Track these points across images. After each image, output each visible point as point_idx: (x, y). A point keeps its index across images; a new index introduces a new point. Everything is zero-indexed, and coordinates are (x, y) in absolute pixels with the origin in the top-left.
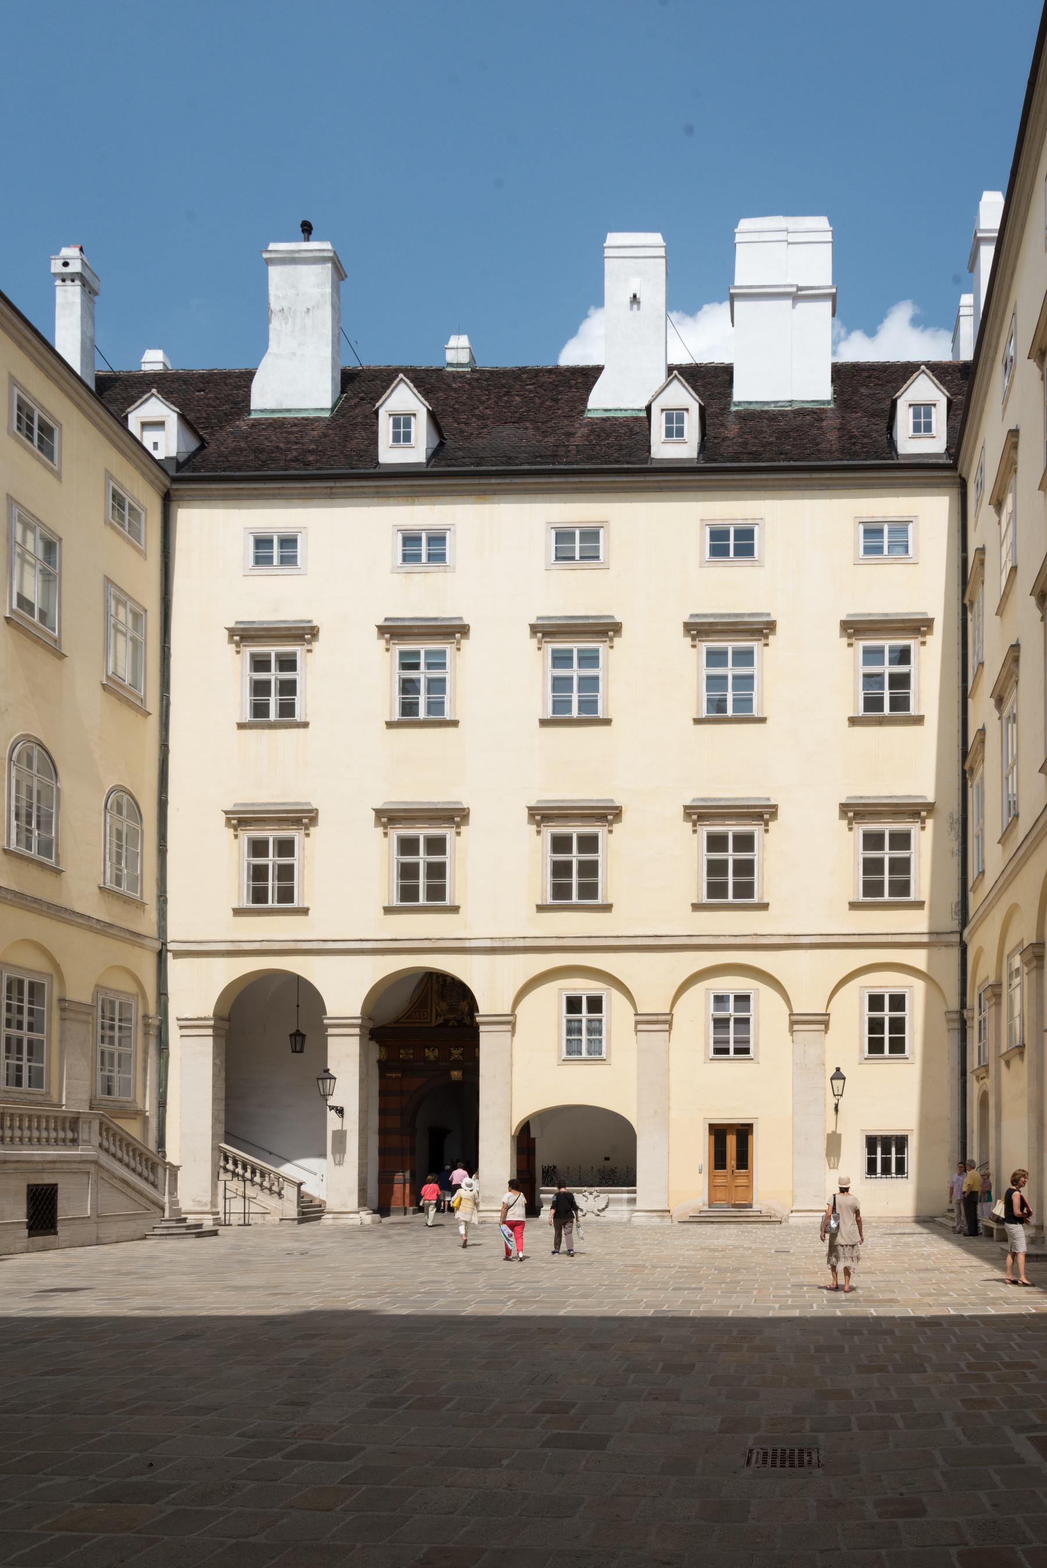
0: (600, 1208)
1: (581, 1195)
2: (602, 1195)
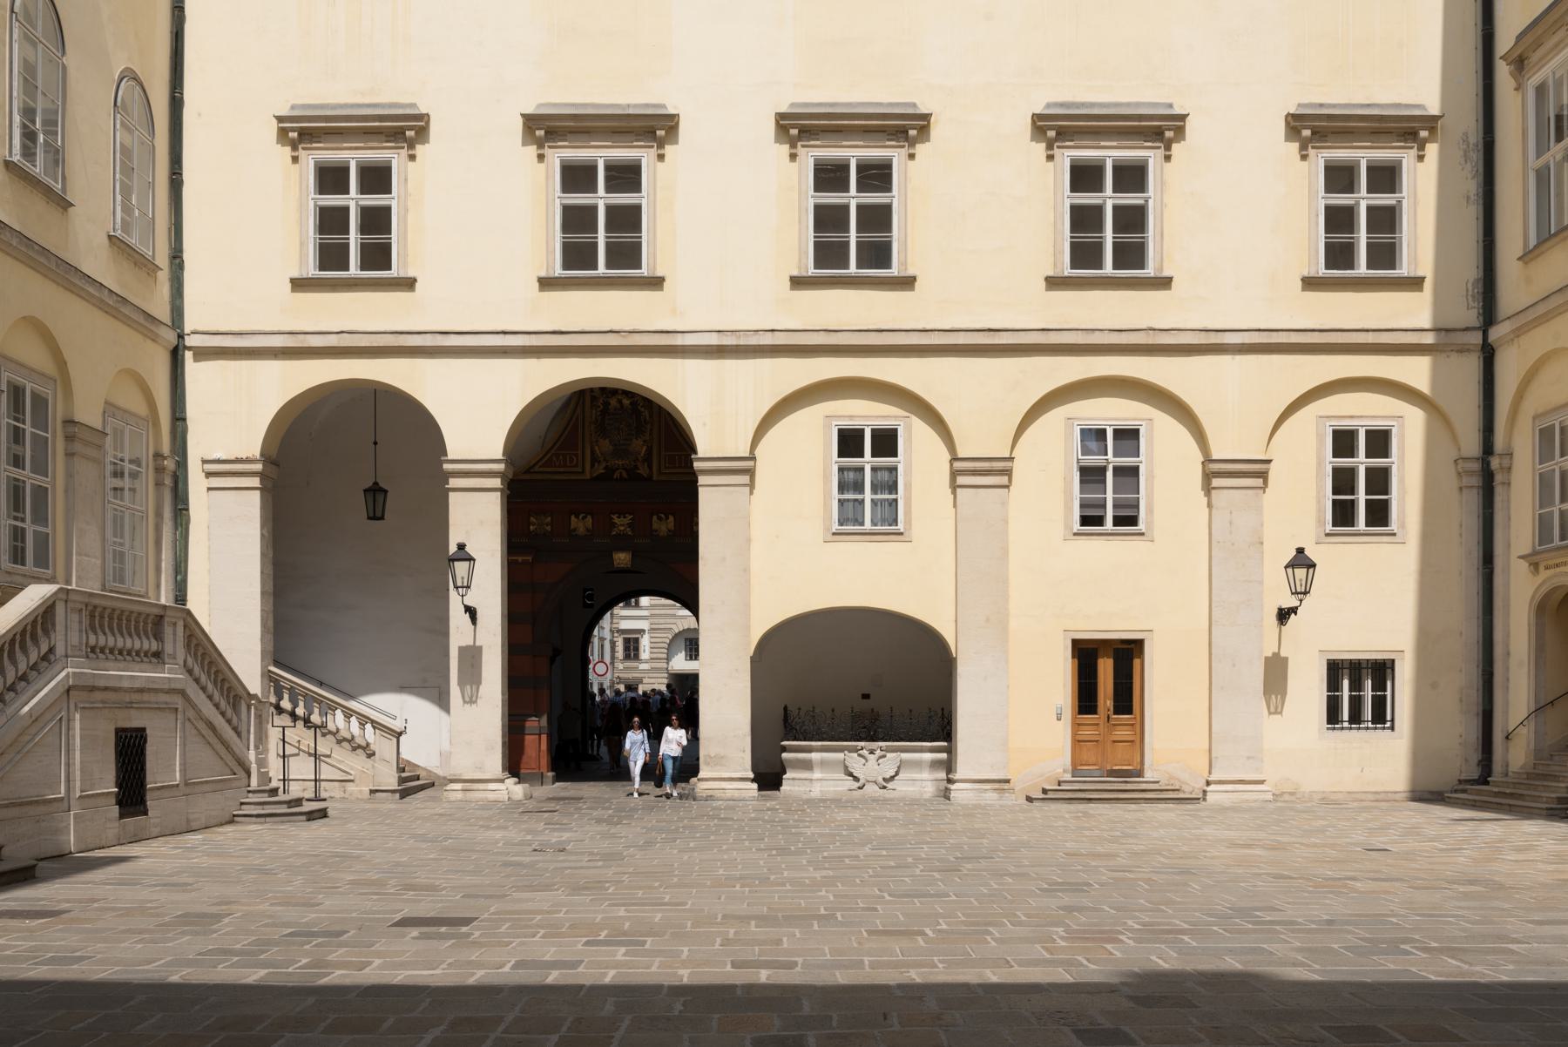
1: (855, 755)
2: (889, 755)
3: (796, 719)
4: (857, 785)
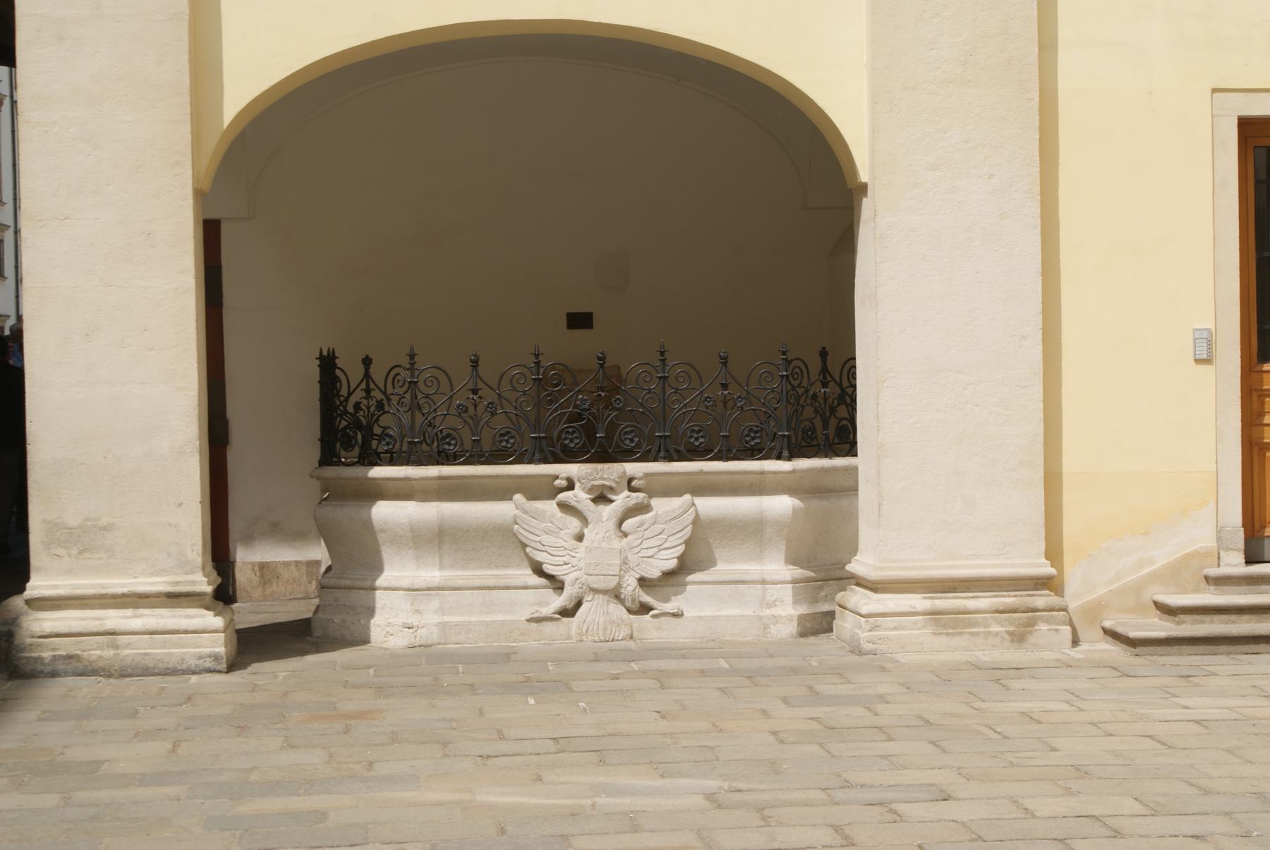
0: (655, 573)
1: (550, 507)
2: (662, 506)
3: (358, 396)
4: (559, 601)
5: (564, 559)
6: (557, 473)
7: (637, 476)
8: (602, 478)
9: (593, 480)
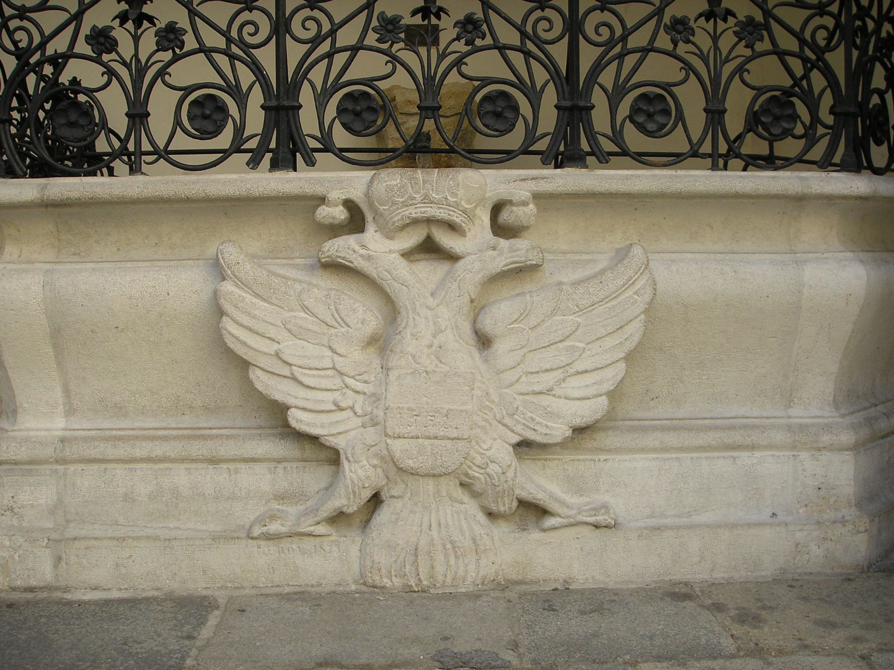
5: (336, 395)
6: (319, 190)
7: (515, 199)
8: (427, 200)
9: (405, 205)
